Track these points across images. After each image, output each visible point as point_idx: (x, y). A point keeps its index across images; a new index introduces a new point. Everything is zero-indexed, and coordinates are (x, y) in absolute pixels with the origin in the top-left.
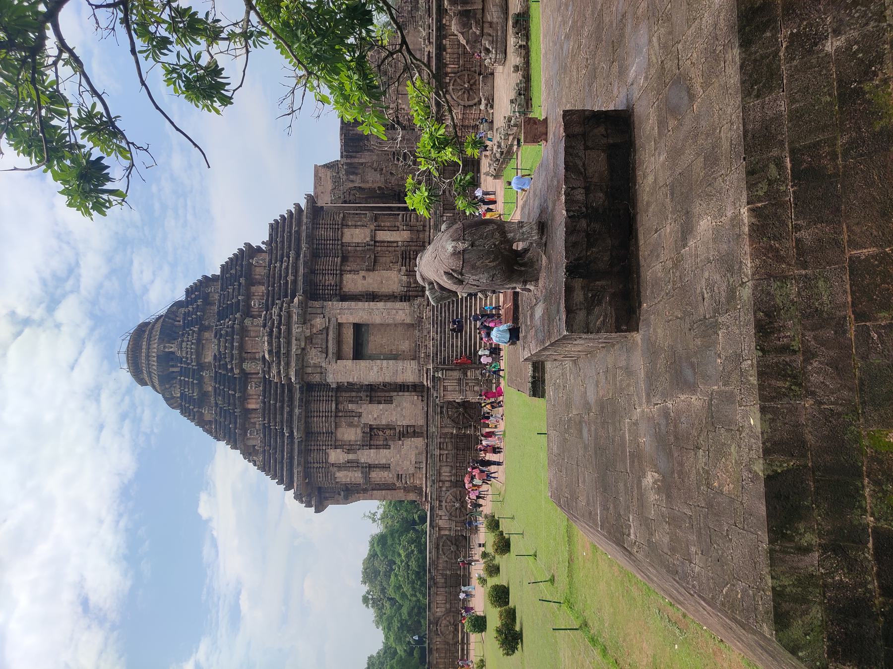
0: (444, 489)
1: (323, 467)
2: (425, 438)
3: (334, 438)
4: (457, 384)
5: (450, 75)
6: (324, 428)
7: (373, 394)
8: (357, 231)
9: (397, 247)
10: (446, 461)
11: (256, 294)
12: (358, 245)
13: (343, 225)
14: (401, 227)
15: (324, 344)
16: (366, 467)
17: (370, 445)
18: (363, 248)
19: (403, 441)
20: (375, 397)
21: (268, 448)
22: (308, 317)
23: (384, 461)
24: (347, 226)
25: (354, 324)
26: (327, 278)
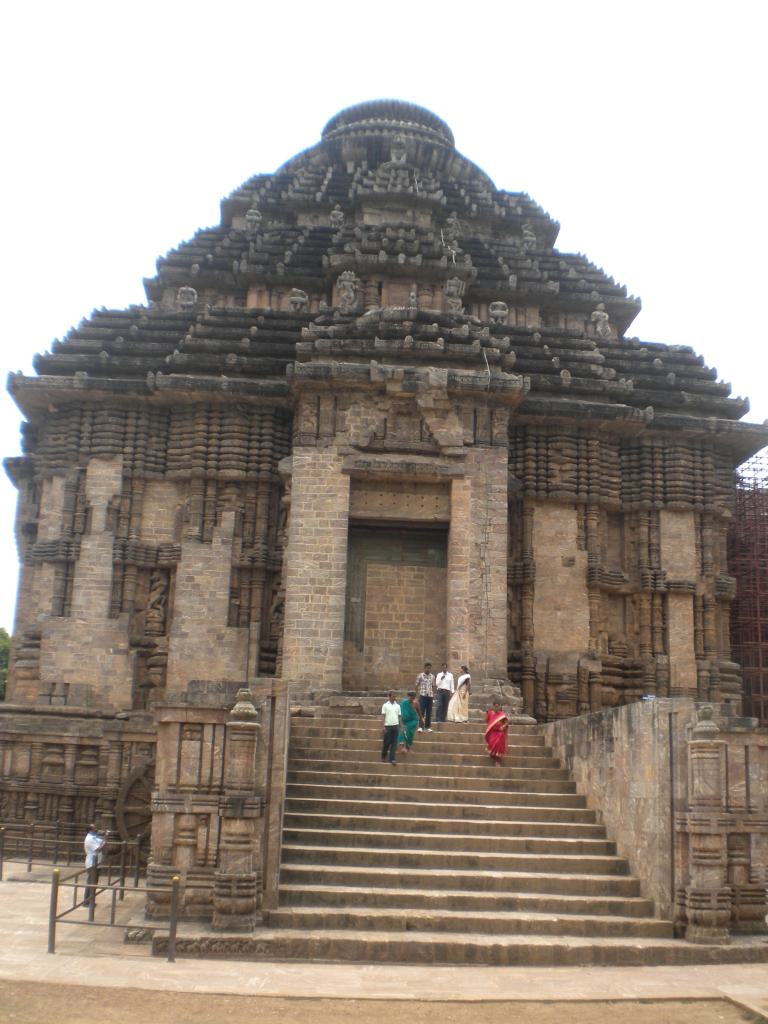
1: (80, 446)
2: (130, 714)
4: (205, 780)
6: (178, 451)
7: (259, 577)
8: (690, 551)
9: (654, 654)
10: (43, 765)
12: (654, 549)
14: (706, 664)
15: (395, 444)
16: (68, 553)
17: (125, 567)
18: (645, 564)
19: (126, 652)
20: (251, 583)
22: (467, 406)
23: (79, 599)
24: (700, 527)
26: (568, 466)
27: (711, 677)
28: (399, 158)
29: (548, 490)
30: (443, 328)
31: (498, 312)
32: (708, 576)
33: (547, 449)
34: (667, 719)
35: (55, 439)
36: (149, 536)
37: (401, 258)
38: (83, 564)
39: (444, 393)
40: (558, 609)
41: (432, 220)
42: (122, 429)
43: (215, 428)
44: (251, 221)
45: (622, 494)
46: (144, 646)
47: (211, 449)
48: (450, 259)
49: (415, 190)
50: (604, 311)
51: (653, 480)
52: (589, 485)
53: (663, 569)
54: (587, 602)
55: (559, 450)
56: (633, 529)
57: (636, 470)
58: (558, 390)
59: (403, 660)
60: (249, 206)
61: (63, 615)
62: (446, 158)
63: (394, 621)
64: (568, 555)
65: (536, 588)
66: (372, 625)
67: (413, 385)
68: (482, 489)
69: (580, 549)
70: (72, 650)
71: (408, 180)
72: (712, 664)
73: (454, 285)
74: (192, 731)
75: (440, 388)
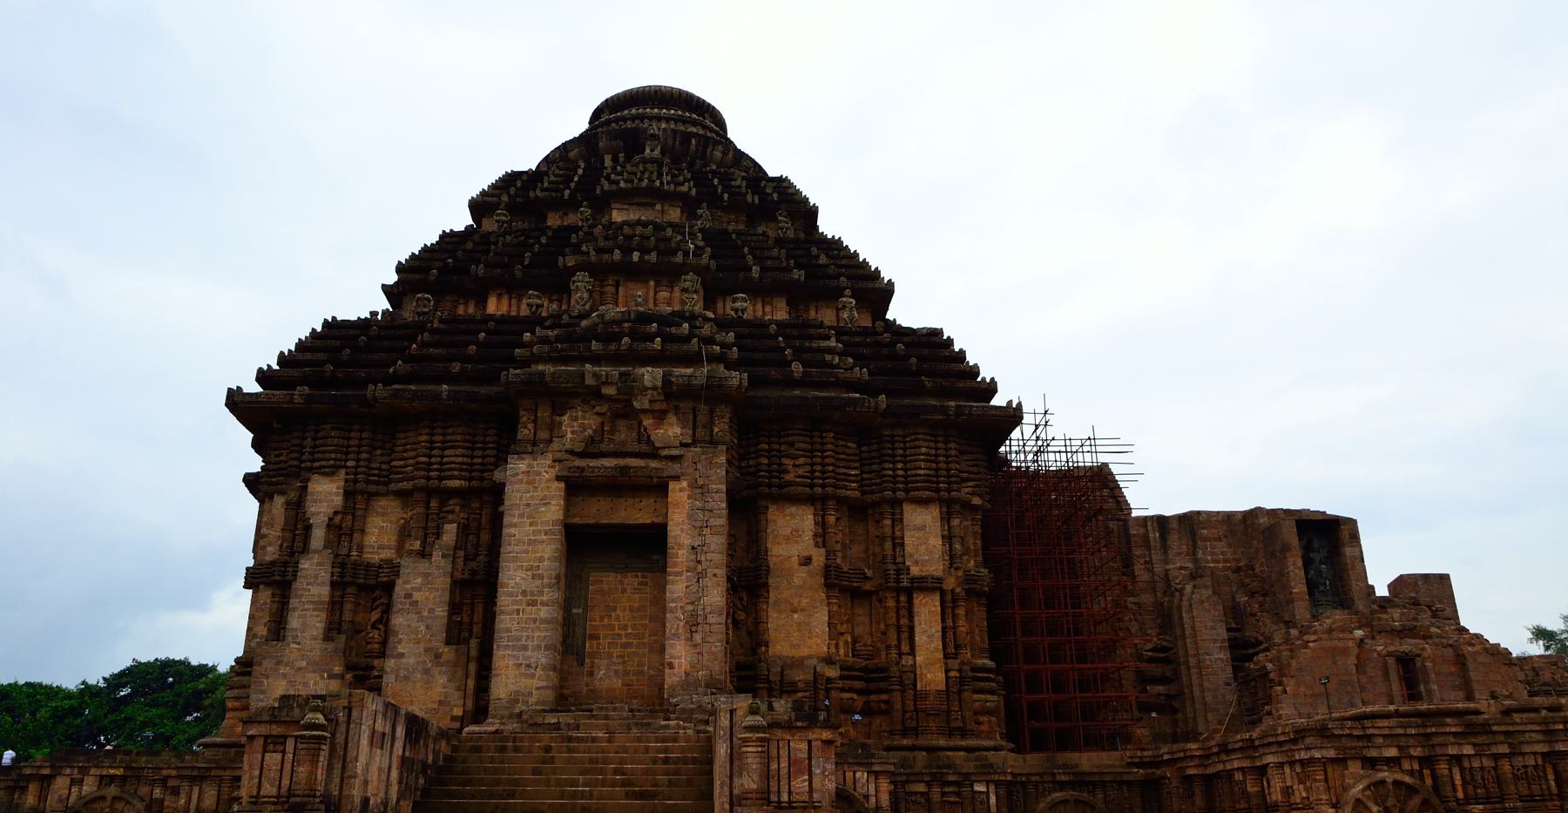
0: (157, 793)
1: (302, 462)
3: (372, 488)
4: (284, 791)
5: (1426, 772)
6: (402, 463)
8: (936, 542)
9: (900, 654)
11: (768, 309)
12: (898, 543)
14: (955, 664)
16: (284, 574)
19: (342, 677)
23: (294, 622)
24: (946, 518)
25: (664, 526)
26: (802, 461)
27: (961, 677)
28: (652, 151)
29: (780, 486)
30: (663, 328)
31: (738, 304)
32: (956, 569)
33: (780, 444)
34: (728, 716)
35: (277, 456)
36: (374, 553)
37: (636, 256)
38: (300, 584)
39: (659, 394)
40: (795, 611)
41: (682, 212)
43: (437, 438)
44: (497, 221)
45: (861, 486)
46: (362, 669)
47: (433, 460)
48: (686, 254)
49: (662, 183)
50: (851, 297)
51: (894, 470)
52: (824, 479)
53: (908, 563)
54: (826, 601)
55: (792, 444)
56: (878, 522)
57: (877, 461)
58: (791, 383)
59: (626, 673)
60: (496, 206)
61: (278, 640)
62: (705, 147)
63: (616, 631)
64: (805, 554)
65: (770, 589)
66: (594, 637)
67: (629, 387)
68: (699, 489)
69: (818, 547)
70: (284, 676)
71: (655, 173)
72: (962, 663)
73: (690, 280)
74: (275, 744)
75: (655, 388)
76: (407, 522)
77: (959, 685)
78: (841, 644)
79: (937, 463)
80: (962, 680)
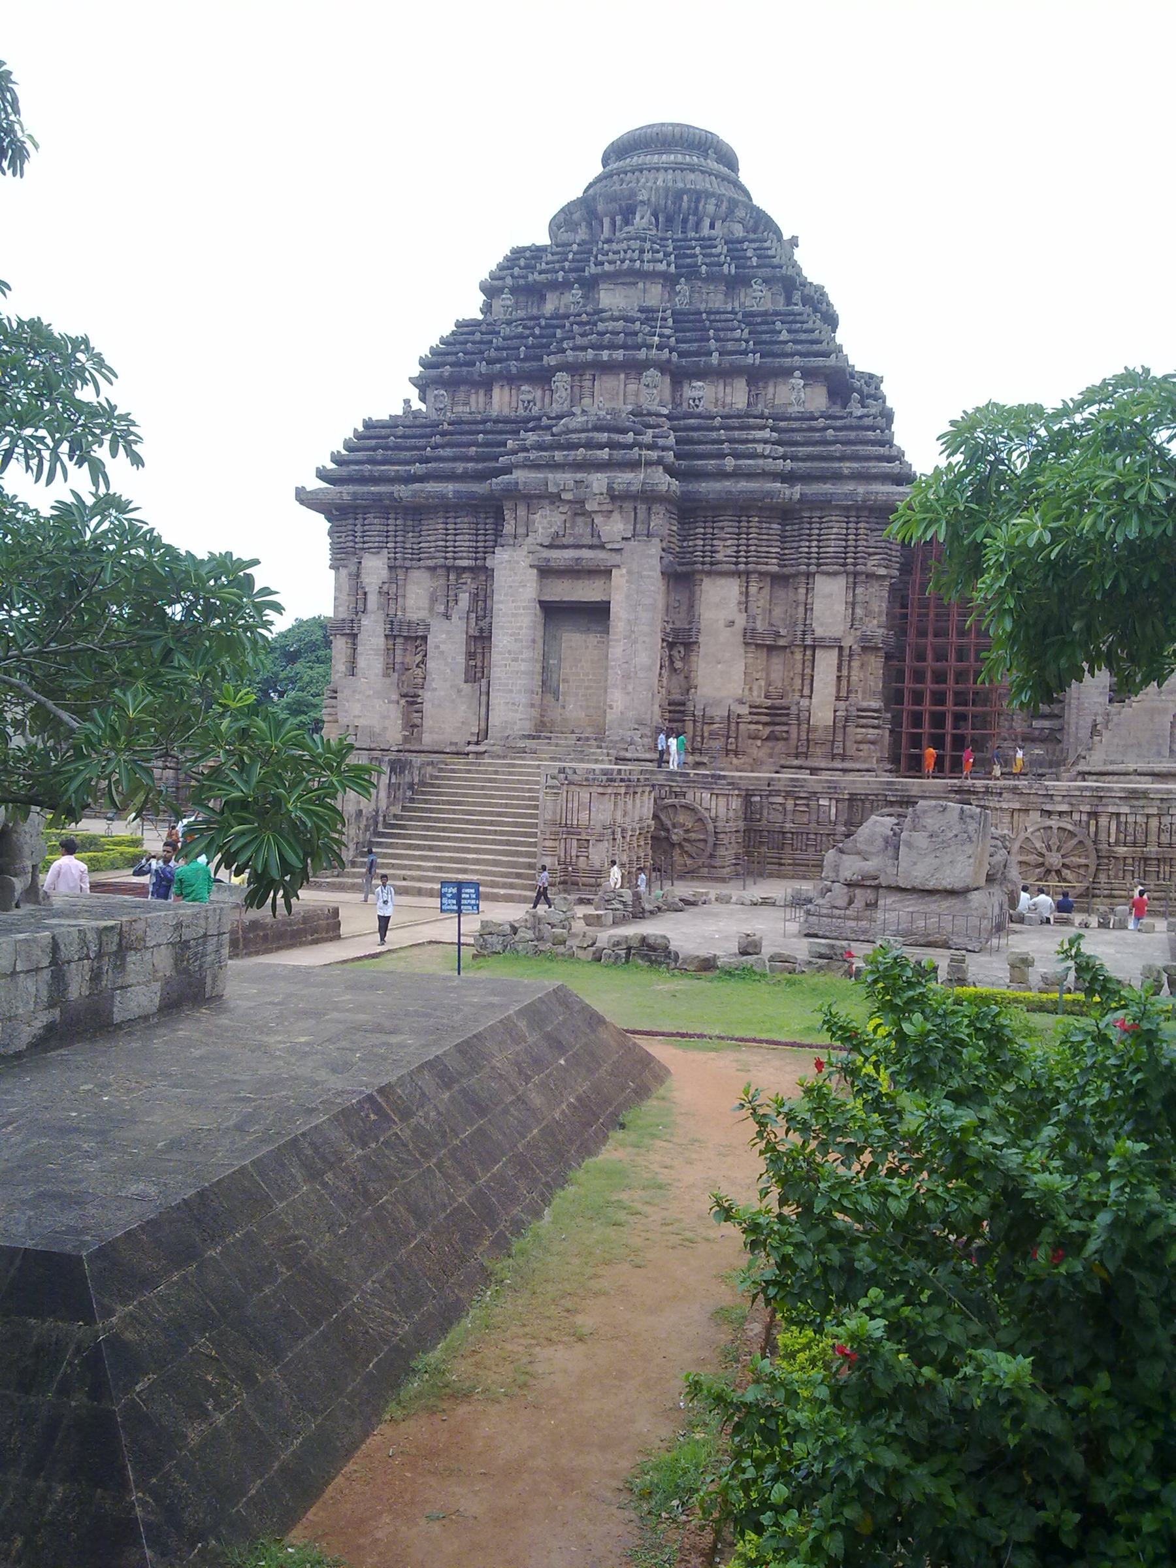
2: (401, 747)
3: (408, 564)
5: (1093, 822)
6: (427, 545)
8: (840, 608)
11: (728, 390)
13: (856, 574)
14: (842, 705)
16: (352, 628)
21: (400, 433)
22: (628, 506)
23: (361, 663)
26: (729, 542)
42: (385, 529)
59: (588, 707)
62: (698, 201)
64: (731, 619)
76: (435, 590)
77: (841, 725)
78: (755, 688)
79: (846, 541)
80: (847, 719)
